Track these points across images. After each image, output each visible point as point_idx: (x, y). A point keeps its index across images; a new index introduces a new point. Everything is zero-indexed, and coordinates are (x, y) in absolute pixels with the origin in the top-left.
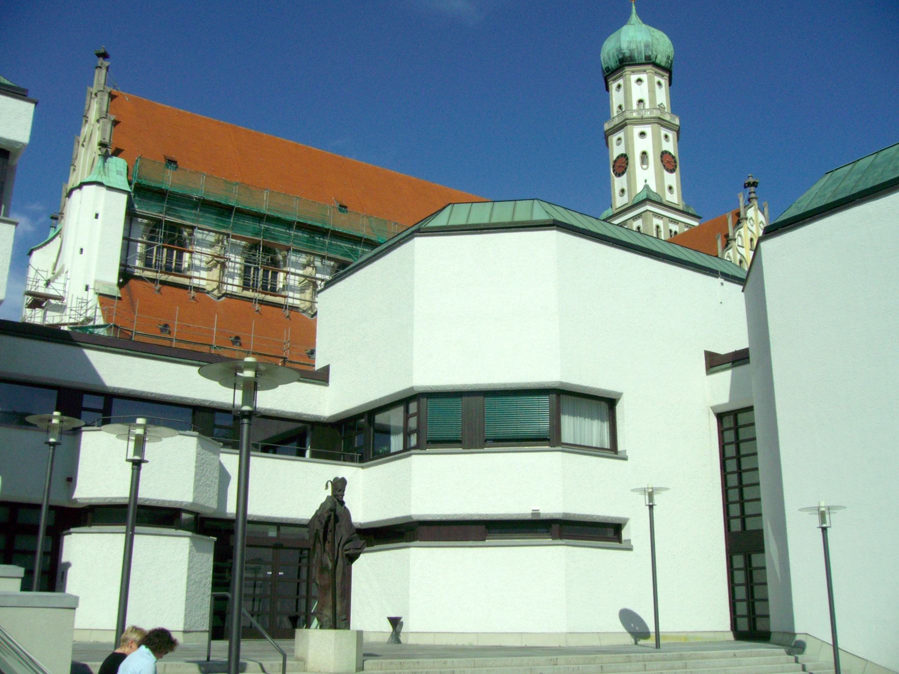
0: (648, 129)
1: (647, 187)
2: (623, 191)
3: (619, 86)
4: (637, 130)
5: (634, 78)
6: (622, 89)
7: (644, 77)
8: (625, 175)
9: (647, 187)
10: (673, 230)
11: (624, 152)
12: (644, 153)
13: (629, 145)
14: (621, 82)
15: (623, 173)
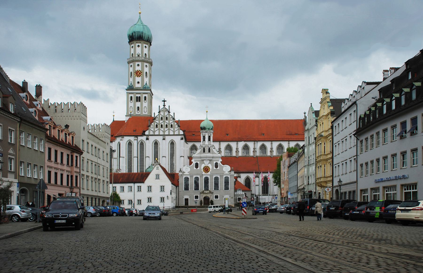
0: (148, 64)
1: (146, 83)
2: (138, 83)
3: (139, 46)
4: (145, 64)
5: (144, 45)
6: (140, 47)
7: (147, 46)
8: (140, 77)
9: (146, 83)
10: (138, 96)
11: (140, 70)
12: (146, 72)
13: (143, 68)
14: (140, 44)
15: (139, 76)
